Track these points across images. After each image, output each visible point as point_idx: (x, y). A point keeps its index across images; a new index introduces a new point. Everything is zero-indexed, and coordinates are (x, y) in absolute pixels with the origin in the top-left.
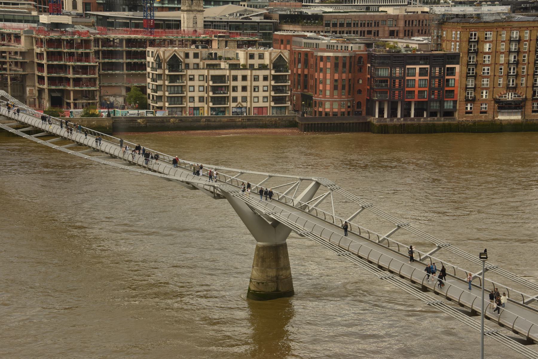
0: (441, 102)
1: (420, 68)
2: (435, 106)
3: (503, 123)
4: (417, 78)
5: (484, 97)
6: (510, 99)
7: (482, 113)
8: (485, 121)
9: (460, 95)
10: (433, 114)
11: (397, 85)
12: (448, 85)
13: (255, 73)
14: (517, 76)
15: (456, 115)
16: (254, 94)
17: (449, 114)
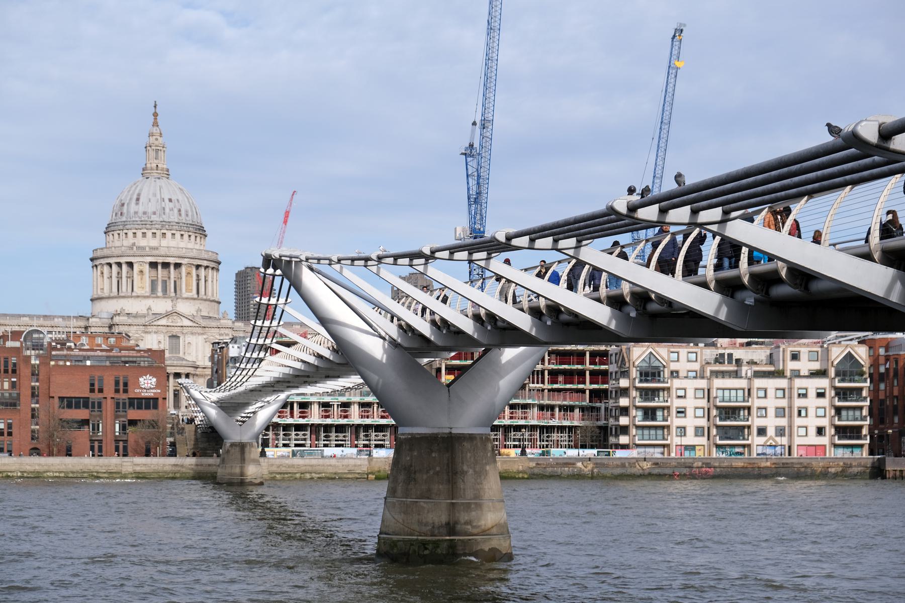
13: (798, 383)
16: (798, 421)
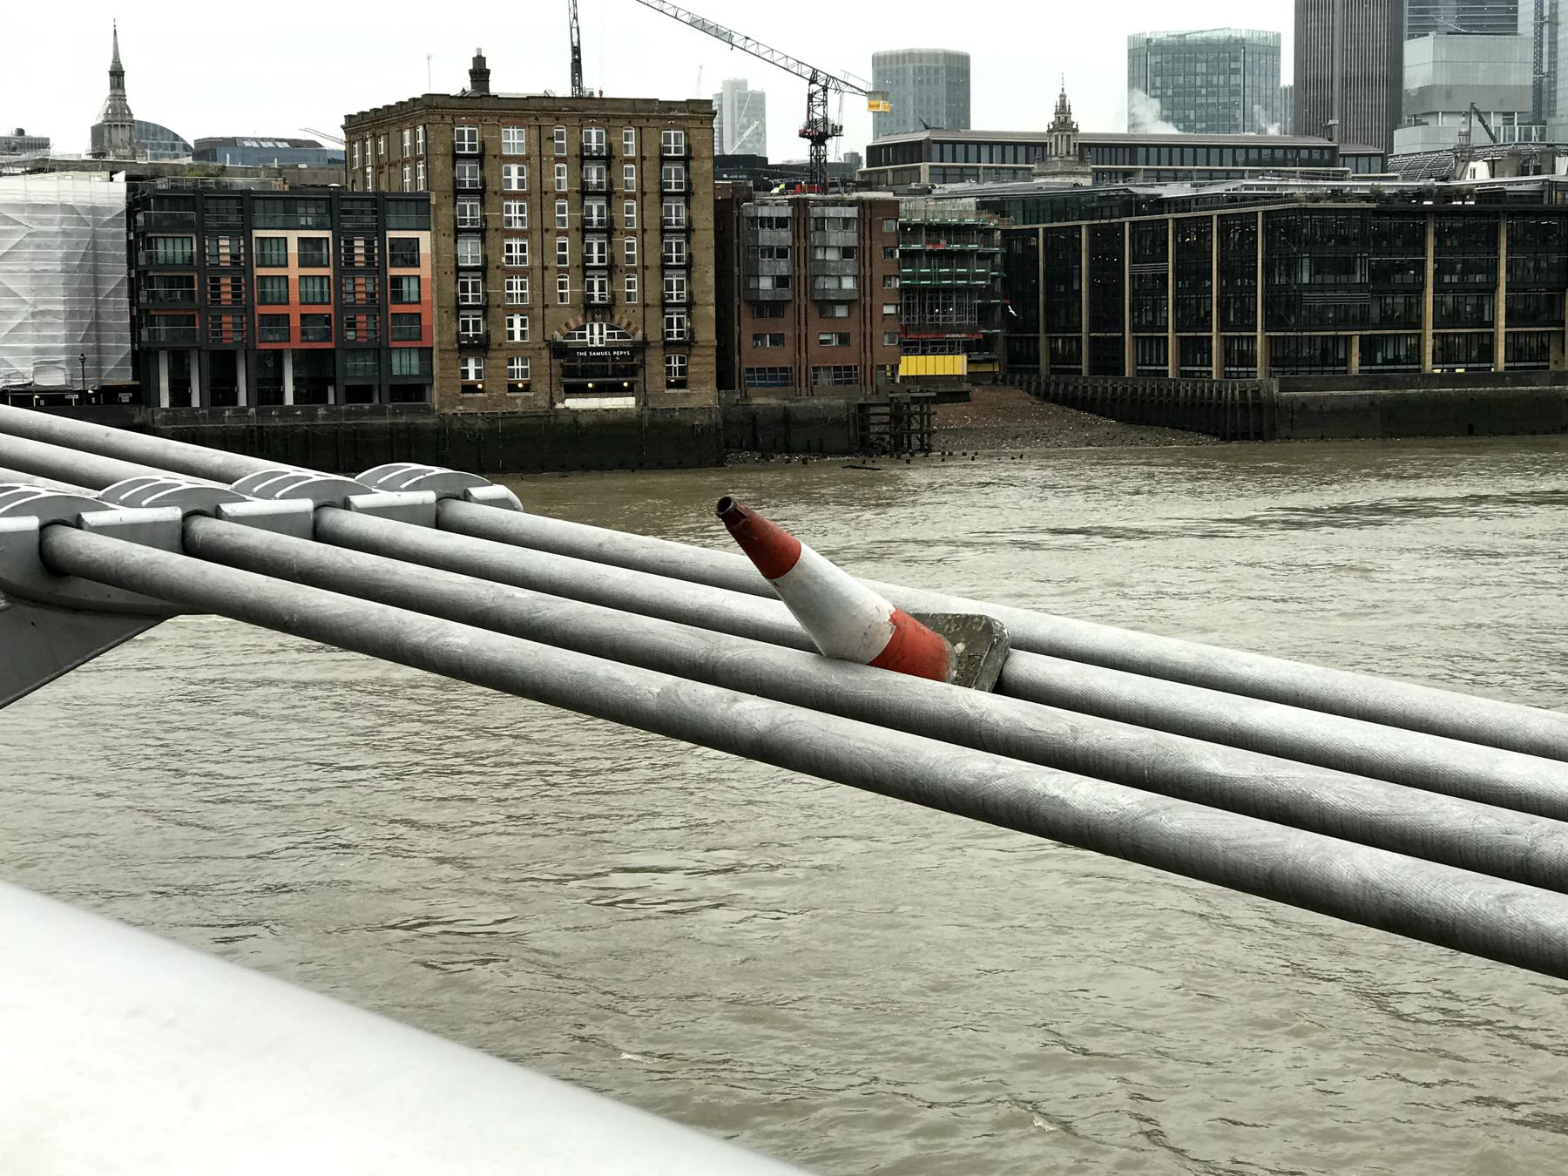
0: (380, 353)
1: (301, 240)
2: (357, 369)
3: (583, 420)
4: (294, 271)
5: (517, 338)
6: (597, 343)
7: (513, 388)
8: (525, 416)
9: (438, 331)
10: (358, 394)
11: (226, 296)
12: (398, 297)
14: (611, 269)
15: (435, 397)
17: (412, 392)
